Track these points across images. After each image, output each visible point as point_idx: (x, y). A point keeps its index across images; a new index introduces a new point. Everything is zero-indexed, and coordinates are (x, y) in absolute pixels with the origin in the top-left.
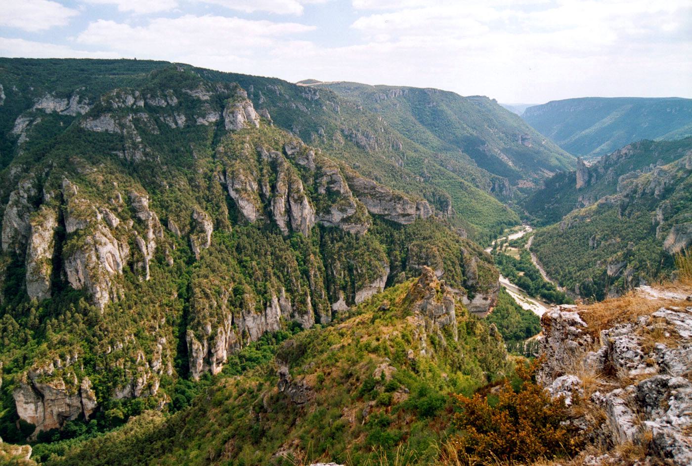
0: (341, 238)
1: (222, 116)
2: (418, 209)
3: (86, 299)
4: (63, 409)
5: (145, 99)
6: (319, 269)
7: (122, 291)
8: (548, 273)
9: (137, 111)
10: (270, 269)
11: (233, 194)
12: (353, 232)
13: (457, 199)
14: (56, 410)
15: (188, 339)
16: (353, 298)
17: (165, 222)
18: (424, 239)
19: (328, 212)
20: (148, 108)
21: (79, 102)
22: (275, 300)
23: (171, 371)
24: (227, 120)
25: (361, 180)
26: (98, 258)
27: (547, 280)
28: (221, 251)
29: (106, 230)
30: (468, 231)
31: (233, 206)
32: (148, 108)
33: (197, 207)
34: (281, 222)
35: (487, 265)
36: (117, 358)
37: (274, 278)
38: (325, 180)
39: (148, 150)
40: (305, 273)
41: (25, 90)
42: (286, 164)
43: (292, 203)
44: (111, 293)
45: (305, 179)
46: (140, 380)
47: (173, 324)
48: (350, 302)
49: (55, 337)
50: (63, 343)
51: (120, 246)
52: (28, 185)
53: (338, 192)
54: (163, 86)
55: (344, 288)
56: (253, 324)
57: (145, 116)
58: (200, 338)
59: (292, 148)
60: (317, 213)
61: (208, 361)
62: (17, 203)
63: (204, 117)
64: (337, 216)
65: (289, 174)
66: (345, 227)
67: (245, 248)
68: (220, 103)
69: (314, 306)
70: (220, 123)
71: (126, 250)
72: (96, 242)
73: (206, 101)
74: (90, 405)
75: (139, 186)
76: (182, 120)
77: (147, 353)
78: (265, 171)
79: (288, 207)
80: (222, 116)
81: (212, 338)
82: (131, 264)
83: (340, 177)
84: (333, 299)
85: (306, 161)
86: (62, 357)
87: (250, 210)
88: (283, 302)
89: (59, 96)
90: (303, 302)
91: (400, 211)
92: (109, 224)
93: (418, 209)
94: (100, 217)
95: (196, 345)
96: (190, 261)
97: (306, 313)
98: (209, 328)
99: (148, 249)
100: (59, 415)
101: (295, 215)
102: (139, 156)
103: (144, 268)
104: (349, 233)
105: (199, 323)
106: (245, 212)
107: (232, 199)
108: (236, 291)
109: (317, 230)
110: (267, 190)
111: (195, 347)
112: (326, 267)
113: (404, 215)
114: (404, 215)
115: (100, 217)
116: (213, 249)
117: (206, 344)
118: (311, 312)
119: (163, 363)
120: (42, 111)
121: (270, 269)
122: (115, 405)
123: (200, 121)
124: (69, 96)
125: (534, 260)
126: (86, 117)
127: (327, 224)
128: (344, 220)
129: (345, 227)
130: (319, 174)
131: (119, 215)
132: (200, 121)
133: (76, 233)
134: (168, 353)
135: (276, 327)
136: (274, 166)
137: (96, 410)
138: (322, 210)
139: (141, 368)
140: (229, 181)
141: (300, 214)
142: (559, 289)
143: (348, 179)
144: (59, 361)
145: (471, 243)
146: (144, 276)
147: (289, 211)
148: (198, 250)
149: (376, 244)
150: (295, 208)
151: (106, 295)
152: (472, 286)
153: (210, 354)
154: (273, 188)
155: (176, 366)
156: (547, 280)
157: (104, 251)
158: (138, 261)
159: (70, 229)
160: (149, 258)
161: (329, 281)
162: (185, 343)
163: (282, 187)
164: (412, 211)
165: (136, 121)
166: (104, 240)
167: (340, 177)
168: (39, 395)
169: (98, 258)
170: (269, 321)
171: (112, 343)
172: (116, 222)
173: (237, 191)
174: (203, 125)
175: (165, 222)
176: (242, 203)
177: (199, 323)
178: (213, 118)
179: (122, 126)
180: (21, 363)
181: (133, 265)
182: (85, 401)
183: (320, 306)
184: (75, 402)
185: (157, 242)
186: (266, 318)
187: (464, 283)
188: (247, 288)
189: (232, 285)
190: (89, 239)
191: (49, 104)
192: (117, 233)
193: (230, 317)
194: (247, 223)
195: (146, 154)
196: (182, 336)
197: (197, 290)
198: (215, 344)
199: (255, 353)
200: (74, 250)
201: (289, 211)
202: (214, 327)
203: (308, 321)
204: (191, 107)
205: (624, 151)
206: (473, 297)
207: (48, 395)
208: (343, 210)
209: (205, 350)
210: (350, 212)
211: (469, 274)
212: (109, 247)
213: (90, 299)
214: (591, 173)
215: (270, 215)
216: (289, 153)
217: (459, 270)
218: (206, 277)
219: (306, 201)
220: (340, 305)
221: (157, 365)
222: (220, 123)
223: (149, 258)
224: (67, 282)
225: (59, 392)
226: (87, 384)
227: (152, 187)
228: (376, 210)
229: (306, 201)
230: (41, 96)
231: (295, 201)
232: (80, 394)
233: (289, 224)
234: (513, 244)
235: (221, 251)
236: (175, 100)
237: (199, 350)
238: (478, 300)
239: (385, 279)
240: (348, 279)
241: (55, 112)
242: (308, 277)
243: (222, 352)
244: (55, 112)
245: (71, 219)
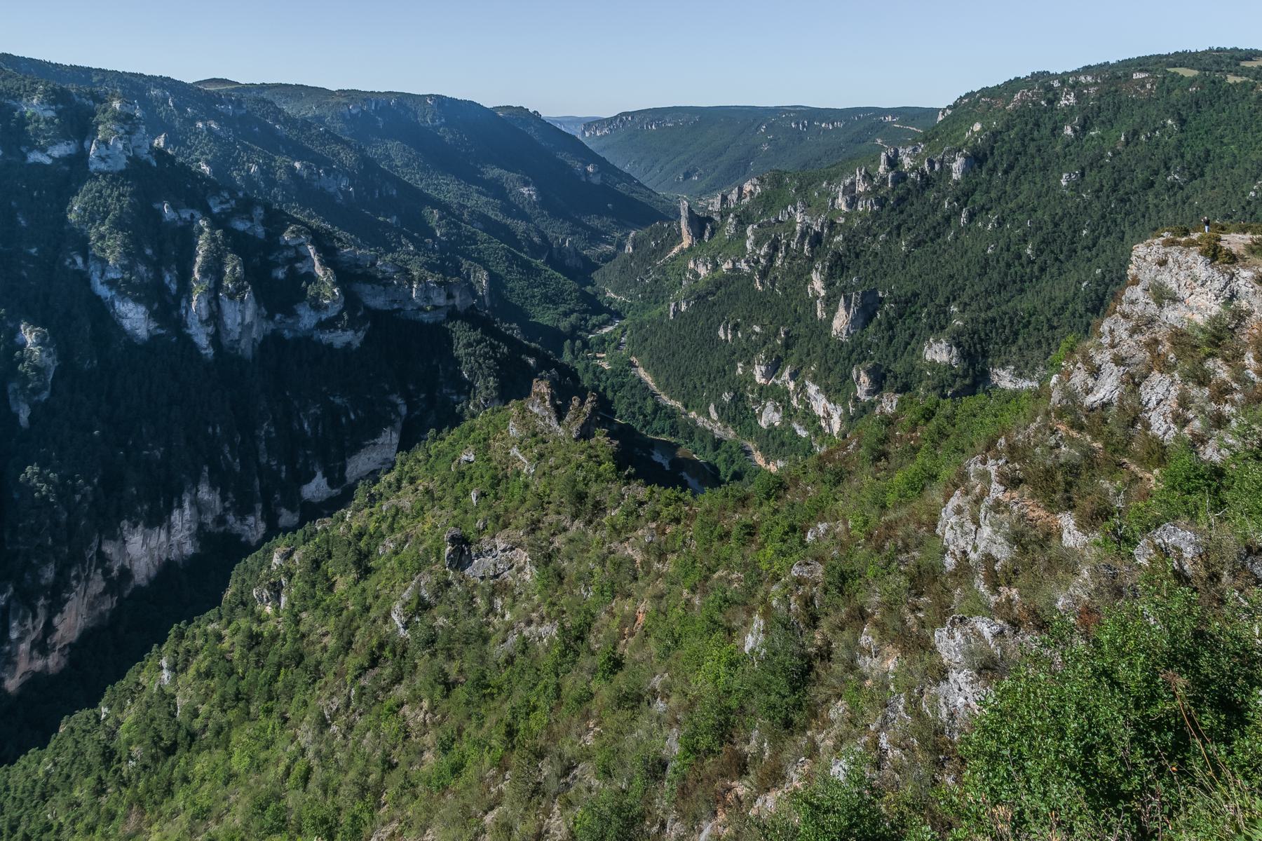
11: (103, 291)
34: (202, 338)
59: (221, 203)
79: (215, 308)
85: (249, 224)
87: (135, 318)
101: (229, 322)
106: (127, 324)
130: (272, 242)
141: (239, 320)
147: (215, 317)
173: (112, 284)
186: (169, 532)
201: (215, 317)
215: (179, 325)
216: (216, 210)
231: (231, 297)
233: (215, 340)
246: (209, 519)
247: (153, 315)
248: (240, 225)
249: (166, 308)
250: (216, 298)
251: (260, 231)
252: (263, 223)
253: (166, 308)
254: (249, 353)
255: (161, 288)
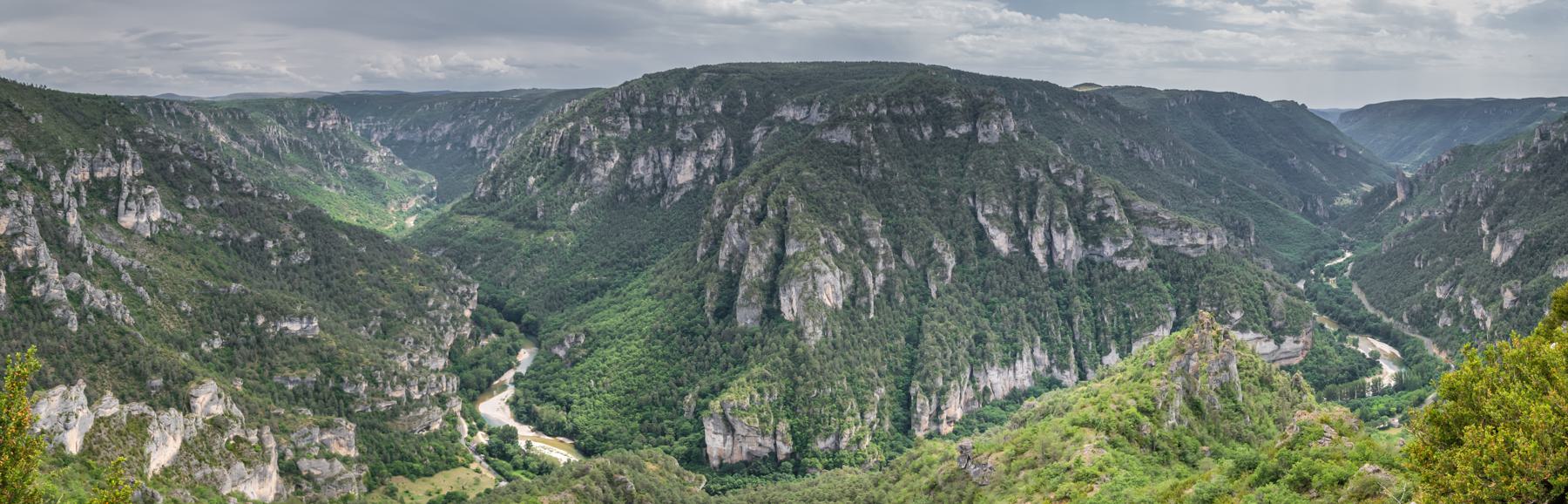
0: (1114, 275)
1: (974, 128)
2: (1210, 238)
3: (797, 333)
4: (754, 448)
5: (889, 106)
6: (1086, 314)
7: (838, 330)
8: (1372, 304)
9: (878, 120)
10: (1022, 313)
11: (982, 220)
12: (1129, 267)
13: (1259, 223)
14: (746, 447)
15: (912, 391)
16: (1129, 350)
17: (898, 251)
18: (1219, 273)
19: (1099, 245)
20: (896, 119)
21: (820, 110)
22: (1026, 353)
23: (887, 426)
24: (980, 133)
25: (1140, 205)
26: (815, 288)
27: (1371, 310)
28: (963, 289)
29: (829, 257)
30: (1274, 260)
31: (981, 234)
32: (896, 119)
33: (937, 235)
34: (1040, 256)
35: (1296, 301)
36: (824, 403)
37: (1028, 326)
38: (1094, 205)
39: (887, 166)
40: (1069, 319)
41: (767, 96)
42: (1048, 186)
43: (1054, 232)
44: (825, 330)
45: (1070, 202)
46: (847, 431)
47: (897, 372)
48: (1124, 352)
49: (756, 370)
50: (765, 377)
51: (843, 278)
52: (753, 199)
53: (1111, 219)
54: (911, 93)
55: (1117, 337)
56: (999, 381)
57: (886, 126)
58: (927, 391)
60: (1085, 246)
61: (935, 420)
62: (739, 218)
63: (953, 129)
64: (1109, 250)
65: (1050, 198)
66: (1119, 262)
67: (992, 286)
68: (975, 113)
69: (1079, 359)
70: (972, 136)
71: (850, 282)
72: (815, 270)
73: (957, 109)
74: (785, 450)
75: (872, 206)
76: (928, 132)
77: (859, 402)
78: (1022, 193)
80: (974, 128)
81: (942, 392)
82: (853, 298)
83: (1112, 201)
84: (1103, 351)
86: (760, 391)
87: (1001, 241)
88: (1037, 353)
89: (800, 104)
90: (1065, 354)
91: (1187, 241)
92: (834, 252)
93: (1210, 238)
94: (823, 240)
95: (921, 400)
96: (925, 297)
97: (1067, 367)
98: (940, 382)
99: (874, 282)
100: (749, 453)
102: (875, 173)
103: (868, 304)
104: (1124, 269)
105: (927, 374)
106: (996, 243)
107: (981, 226)
108: (979, 339)
109: (1084, 265)
110: (1023, 216)
111: (920, 401)
112: (1095, 312)
113: (1193, 247)
114: (1193, 247)
115: (823, 240)
116: (952, 287)
117: (934, 397)
118: (1073, 366)
119: (879, 416)
120: (782, 119)
121: (1022, 313)
122: (815, 455)
123: (950, 133)
124: (810, 104)
125: (1356, 290)
126: (822, 126)
127: (1097, 259)
128: (1121, 254)
129: (1119, 262)
130: (1086, 197)
131: (846, 241)
132: (950, 133)
133: (795, 256)
134: (887, 404)
135: (1027, 384)
136: (1034, 187)
137: (792, 455)
138: (1090, 234)
139: (850, 418)
140: (979, 205)
142: (1385, 320)
143: (1124, 203)
144: (757, 396)
145: (1278, 276)
146: (868, 313)
147: (1049, 243)
148: (933, 288)
149: (1160, 284)
150: (1058, 240)
151: (819, 331)
152: (1280, 329)
153: (939, 411)
154: (1031, 214)
155: (894, 420)
156: (1371, 310)
157: (820, 279)
158: (862, 295)
159: (790, 252)
160: (874, 293)
161: (1097, 332)
162: (909, 395)
163: (1041, 217)
164: (1202, 241)
165: (877, 133)
166: (824, 267)
167: (1112, 201)
168: (730, 429)
169: (815, 288)
170: (1019, 376)
171: (819, 386)
172: (840, 247)
173: (987, 216)
174: (952, 138)
175: (898, 251)
176: (992, 232)
177: (927, 374)
178: (963, 129)
179: (859, 137)
180: (715, 391)
181: (854, 296)
182: (779, 444)
183: (1086, 360)
184: (768, 442)
185: (886, 272)
187: (1269, 325)
188: (992, 336)
189: (974, 332)
190: (806, 266)
191: (789, 113)
192: (840, 260)
193: (968, 370)
194: (997, 253)
195: (883, 171)
196: (907, 388)
197: (929, 337)
198: (945, 401)
199: (997, 413)
200: (788, 278)
201: (1049, 243)
202: (946, 380)
203: (1069, 377)
204: (941, 117)
205: (1445, 157)
206: (1282, 341)
207: (739, 429)
208: (1116, 242)
209: (934, 406)
210: (1126, 245)
211: (1275, 314)
212: (830, 276)
213: (800, 333)
214: (1411, 186)
217: (1262, 309)
218: (941, 320)
219: (1071, 231)
220: (1112, 359)
221: (871, 417)
222: (972, 136)
223: (874, 293)
224: (779, 311)
225: (750, 429)
226: (783, 426)
227: (887, 211)
228: (1159, 241)
229: (1071, 231)
230: (782, 103)
231: (1058, 230)
232: (775, 436)
233: (1050, 258)
234: (1331, 272)
235: (963, 289)
236: (922, 108)
237: (924, 407)
238: (1289, 344)
239: (1170, 325)
240: (1122, 326)
241: (794, 120)
242: (1071, 324)
243: (955, 409)
244: (794, 120)
245: (792, 241)
246: (1041, 369)
247: (1011, 240)
248: (1069, 183)
249: (1021, 237)
250: (1050, 231)
251: (1080, 187)
252: (1083, 181)
253: (1021, 237)
254: (1071, 270)
255: (1018, 223)
